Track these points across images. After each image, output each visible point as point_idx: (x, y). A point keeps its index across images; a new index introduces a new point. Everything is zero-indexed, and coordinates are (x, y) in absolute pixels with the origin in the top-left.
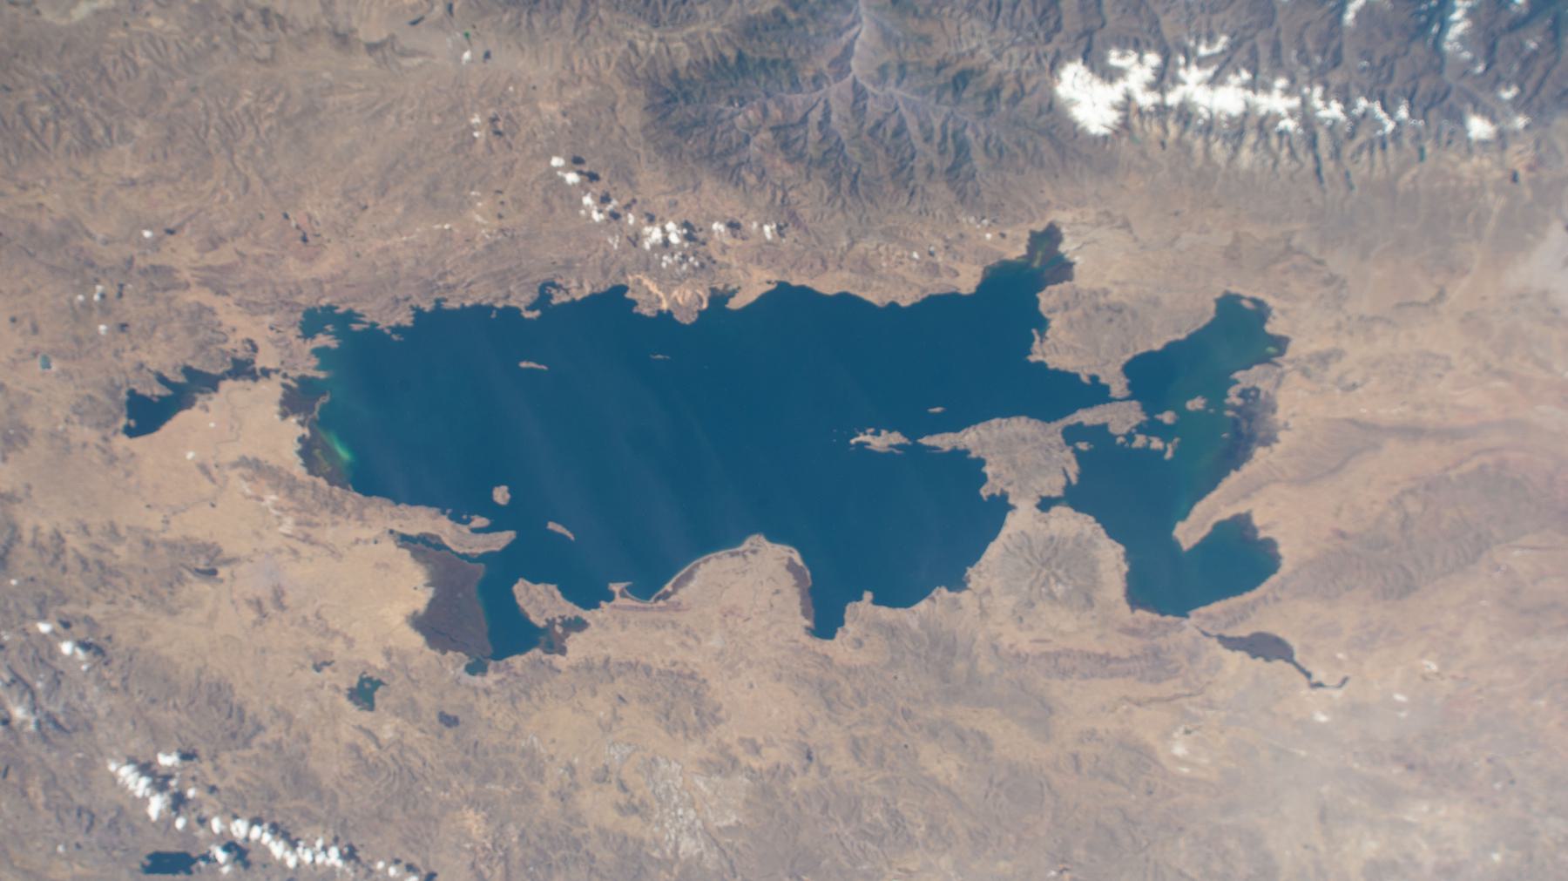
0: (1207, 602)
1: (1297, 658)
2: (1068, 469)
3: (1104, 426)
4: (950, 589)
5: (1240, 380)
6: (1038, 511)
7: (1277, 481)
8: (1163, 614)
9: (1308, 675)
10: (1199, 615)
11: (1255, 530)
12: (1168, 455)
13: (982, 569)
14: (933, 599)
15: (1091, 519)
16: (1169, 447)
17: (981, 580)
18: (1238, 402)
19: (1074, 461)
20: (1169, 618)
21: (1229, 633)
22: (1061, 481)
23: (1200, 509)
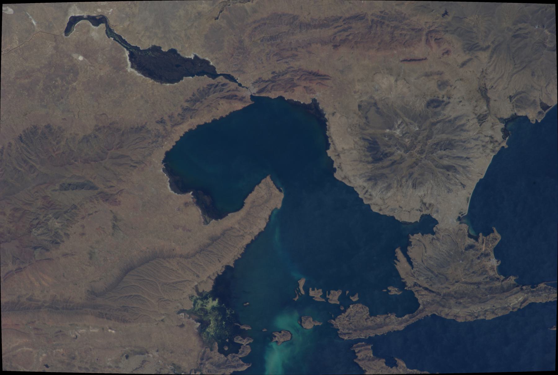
0: (234, 115)
1: (127, 53)
2: (407, 265)
3: (372, 314)
4: (526, 118)
5: (242, 362)
6: (434, 216)
7: (187, 257)
8: (281, 98)
9: (110, 32)
10: (242, 99)
11: (199, 202)
12: (302, 283)
13: (490, 146)
14: (544, 107)
15: (375, 209)
16: (303, 292)
17: (490, 133)
18: (238, 340)
19: (402, 274)
20: (273, 95)
21: (206, 80)
22: (412, 252)
23: (262, 225)
